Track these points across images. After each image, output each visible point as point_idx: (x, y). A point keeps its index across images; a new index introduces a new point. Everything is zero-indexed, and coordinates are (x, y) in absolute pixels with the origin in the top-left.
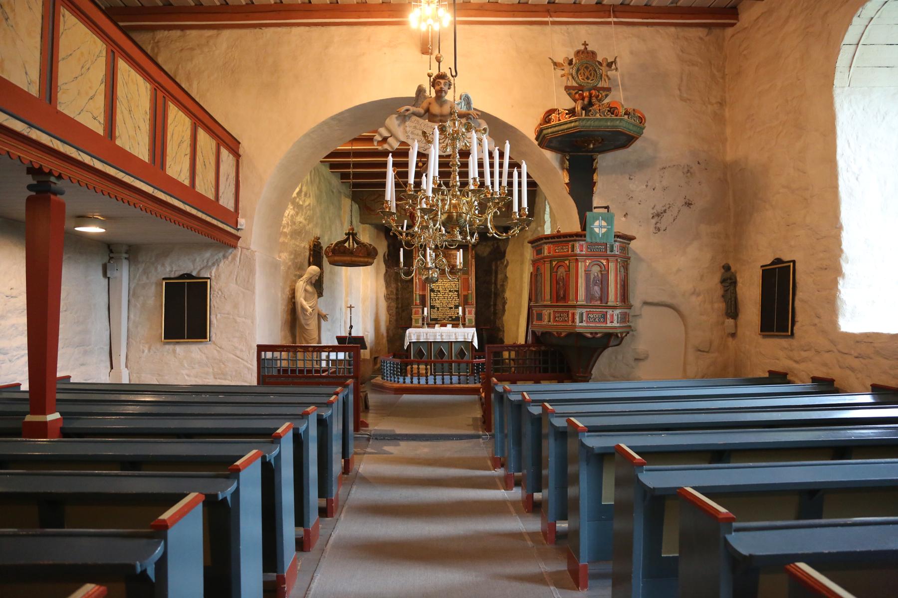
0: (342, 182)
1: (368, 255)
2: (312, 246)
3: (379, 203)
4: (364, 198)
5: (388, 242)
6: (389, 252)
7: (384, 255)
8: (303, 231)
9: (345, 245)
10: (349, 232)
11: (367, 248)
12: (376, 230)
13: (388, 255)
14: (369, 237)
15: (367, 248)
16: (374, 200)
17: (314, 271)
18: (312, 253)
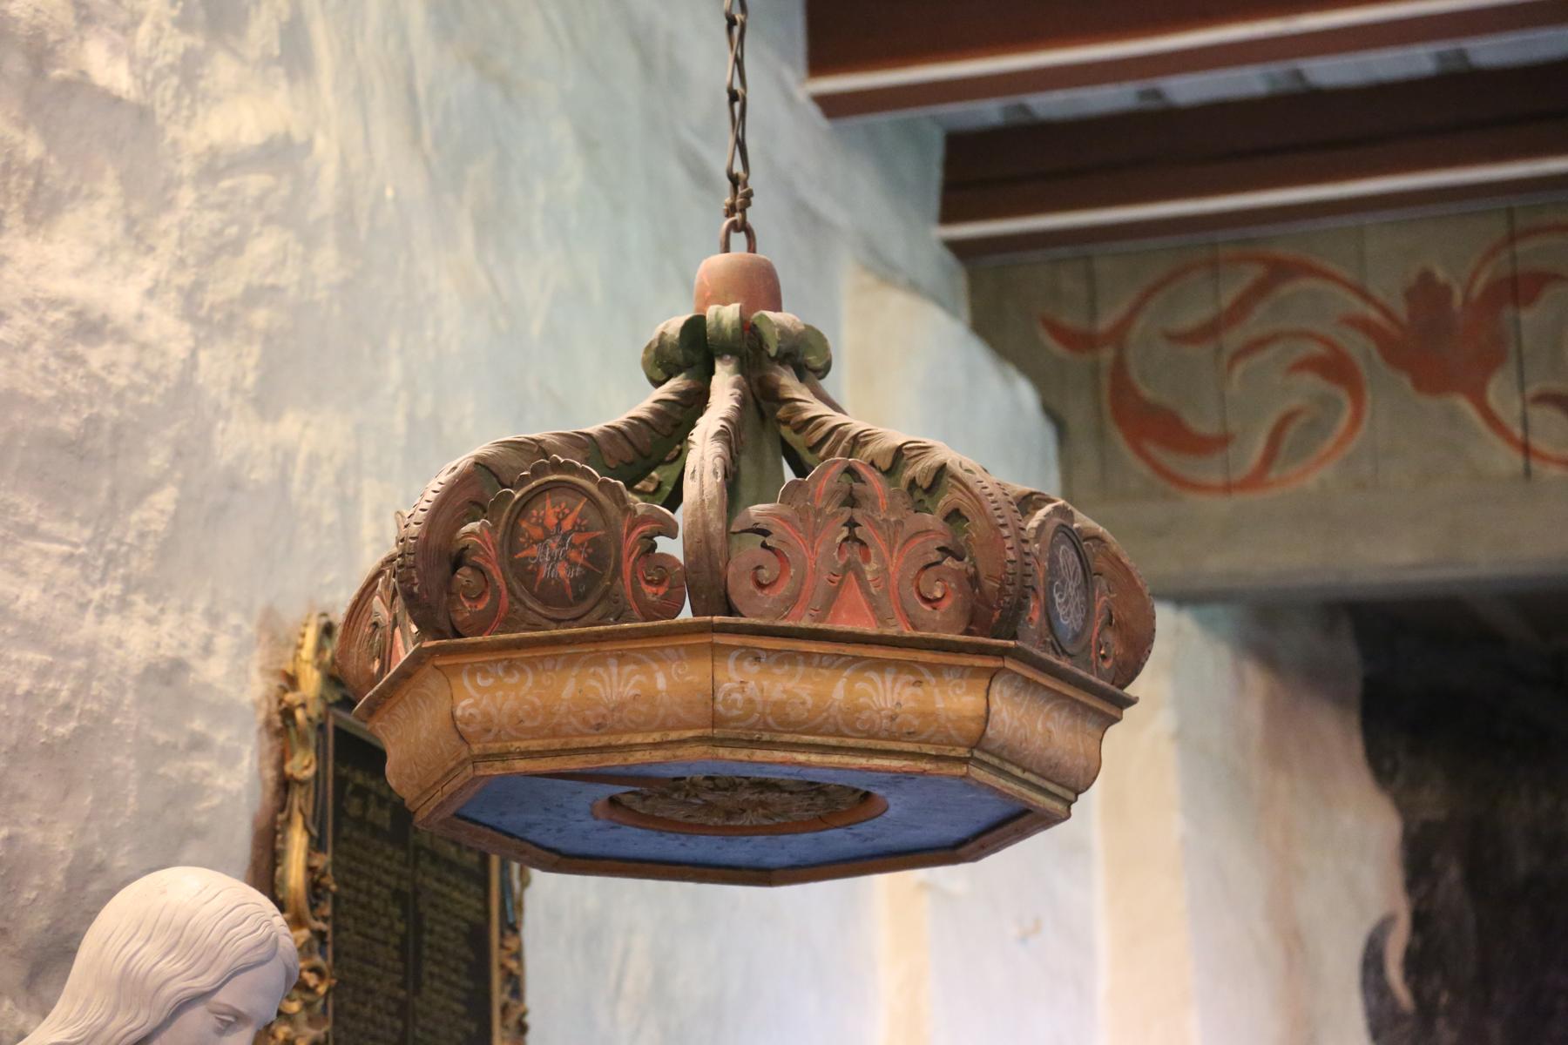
0: (832, 106)
1: (975, 620)
2: (311, 681)
3: (1270, 353)
4: (1104, 323)
5: (1404, 809)
6: (1420, 921)
7: (1373, 961)
8: (158, 459)
9: (680, 557)
10: (695, 328)
11: (955, 516)
12: (1256, 679)
13: (1415, 964)
14: (1180, 735)
15: (955, 516)
16: (1209, 331)
17: (180, 938)
18: (302, 765)
